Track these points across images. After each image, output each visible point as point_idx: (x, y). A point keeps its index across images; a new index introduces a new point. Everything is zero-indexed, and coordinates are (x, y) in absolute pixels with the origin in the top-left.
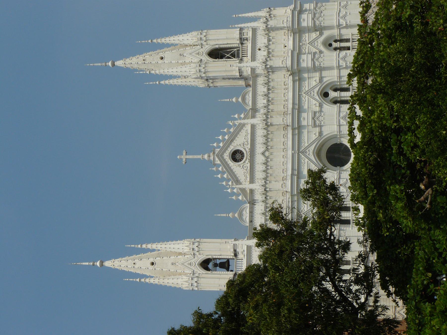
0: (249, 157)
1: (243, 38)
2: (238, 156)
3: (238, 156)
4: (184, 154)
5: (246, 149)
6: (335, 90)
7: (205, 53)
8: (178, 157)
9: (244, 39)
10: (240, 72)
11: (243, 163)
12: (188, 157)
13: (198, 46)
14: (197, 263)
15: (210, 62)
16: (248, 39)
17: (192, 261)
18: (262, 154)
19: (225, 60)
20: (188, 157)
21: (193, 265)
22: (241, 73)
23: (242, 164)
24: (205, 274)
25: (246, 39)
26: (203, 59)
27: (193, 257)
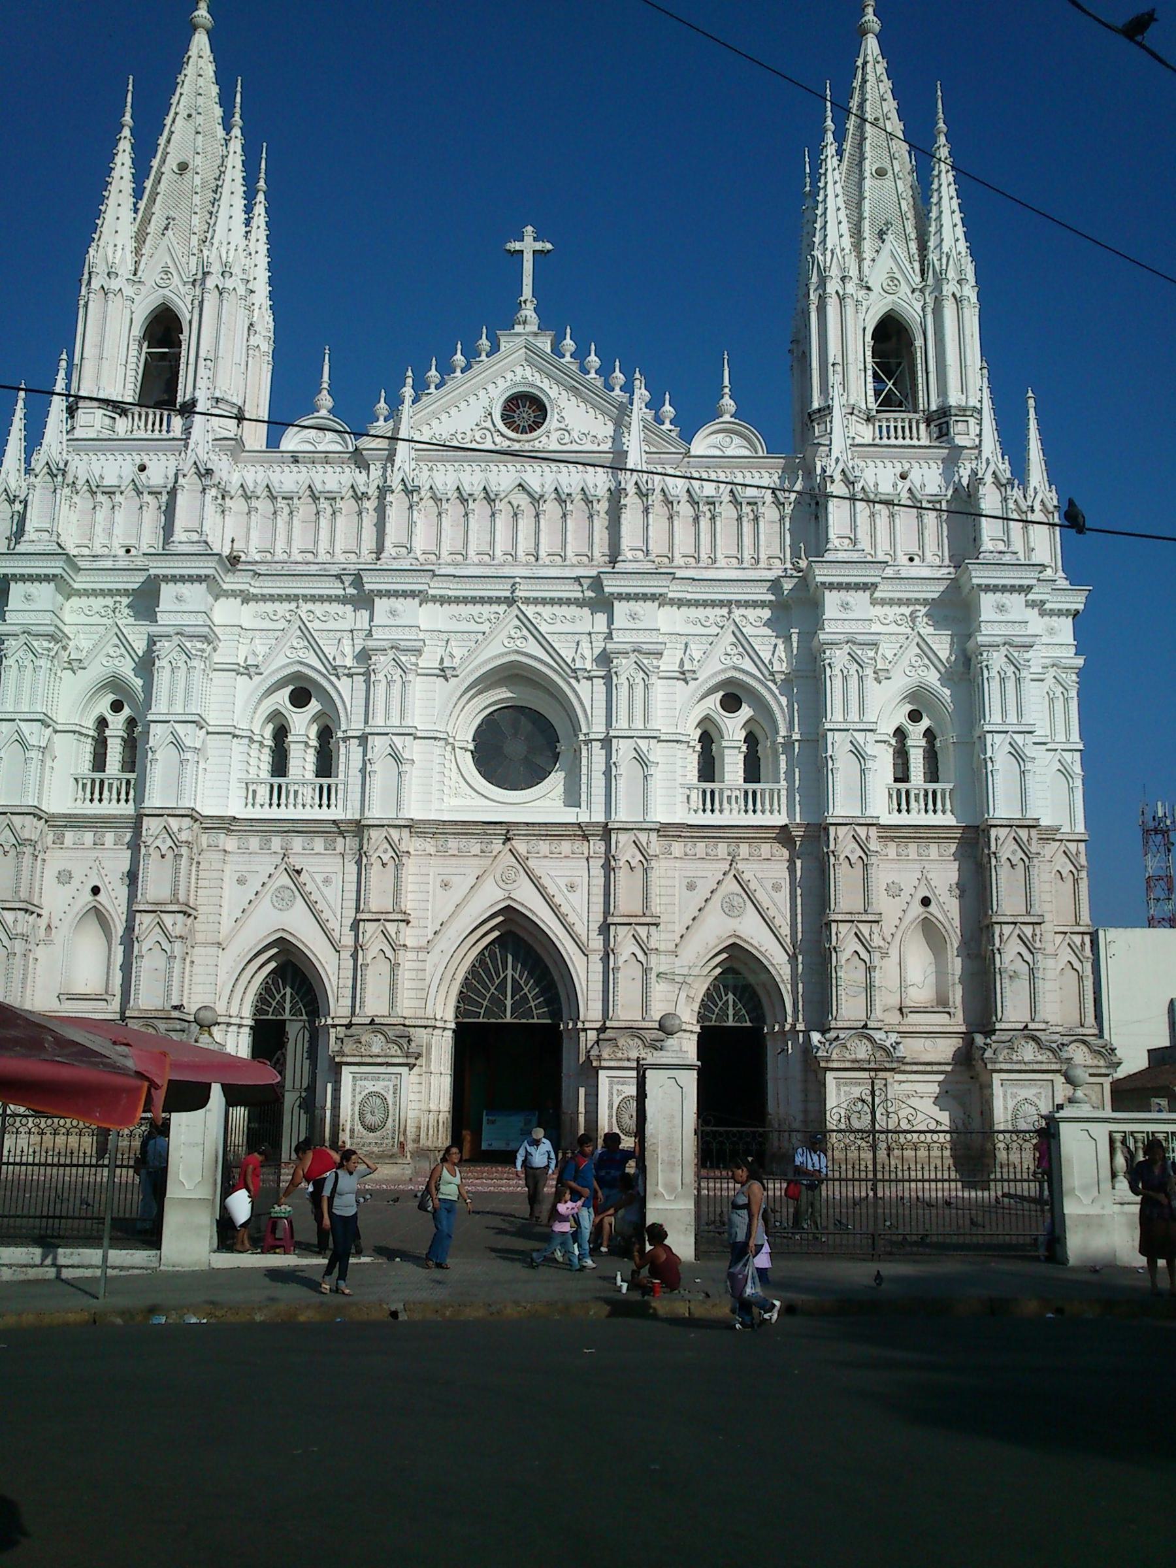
0: (516, 446)
1: (947, 423)
2: (525, 414)
3: (525, 415)
4: (539, 246)
5: (547, 439)
6: (751, 739)
7: (894, 302)
8: (530, 229)
9: (944, 426)
10: (823, 413)
11: (499, 431)
12: (528, 259)
13: (918, 279)
14: (166, 292)
15: (861, 316)
16: (945, 438)
17: (176, 279)
18: (520, 485)
19: (869, 366)
20: (528, 259)
21: (162, 281)
22: (818, 415)
23: (494, 426)
24: (131, 319)
25: (944, 431)
26: (873, 295)
27: (185, 280)
